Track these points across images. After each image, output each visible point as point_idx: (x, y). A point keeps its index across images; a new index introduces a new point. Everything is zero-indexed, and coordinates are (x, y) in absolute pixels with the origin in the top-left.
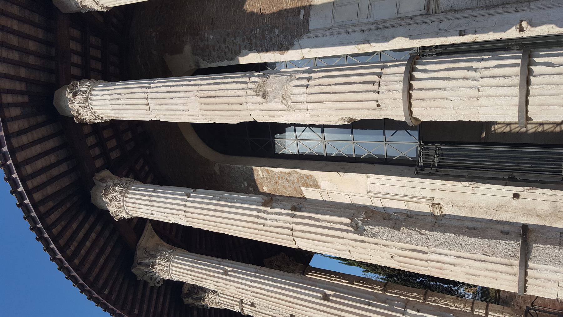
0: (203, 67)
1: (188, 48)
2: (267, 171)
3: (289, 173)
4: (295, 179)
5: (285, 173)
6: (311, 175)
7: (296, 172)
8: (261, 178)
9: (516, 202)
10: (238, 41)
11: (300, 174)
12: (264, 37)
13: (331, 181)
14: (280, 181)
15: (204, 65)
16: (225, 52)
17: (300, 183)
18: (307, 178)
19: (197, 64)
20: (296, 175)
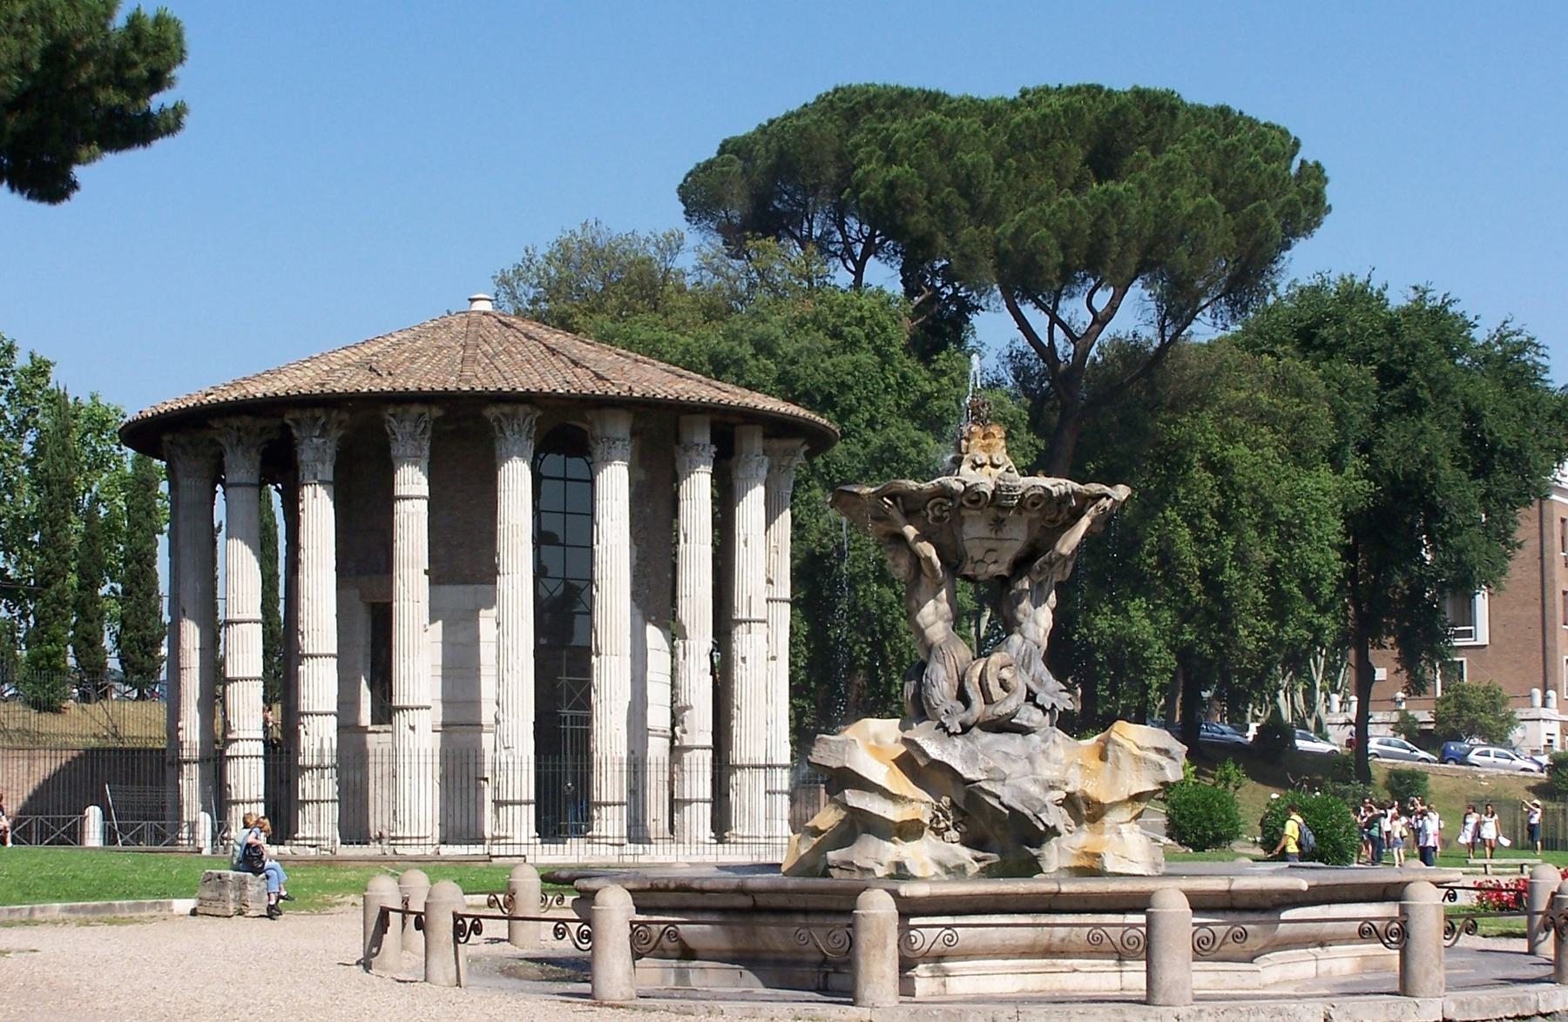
1: (642, 475)
12: (645, 576)
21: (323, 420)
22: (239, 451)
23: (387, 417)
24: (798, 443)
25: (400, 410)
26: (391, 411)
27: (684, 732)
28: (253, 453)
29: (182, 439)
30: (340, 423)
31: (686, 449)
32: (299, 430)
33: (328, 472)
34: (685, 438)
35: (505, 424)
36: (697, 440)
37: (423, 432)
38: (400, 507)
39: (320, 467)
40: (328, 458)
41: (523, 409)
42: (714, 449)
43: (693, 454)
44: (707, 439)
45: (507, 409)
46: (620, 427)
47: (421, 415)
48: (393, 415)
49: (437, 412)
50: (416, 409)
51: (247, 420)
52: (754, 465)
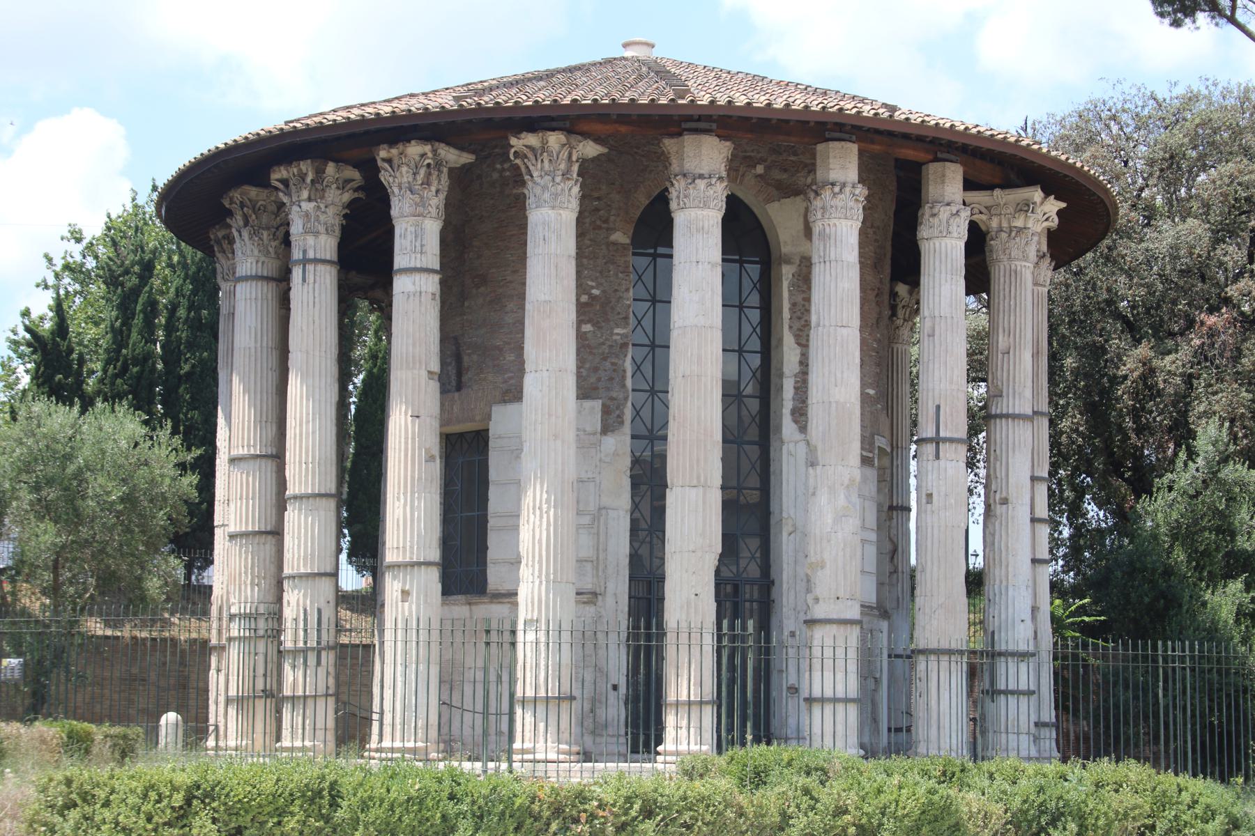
0: (784, 271)
2: (624, 346)
3: (624, 386)
4: (614, 395)
5: (624, 378)
6: (622, 423)
7: (626, 399)
8: (612, 329)
11: (624, 405)
13: (616, 454)
14: (608, 364)
16: (799, 318)
17: (609, 403)
18: (619, 416)
19: (788, 262)
20: (621, 396)
22: (245, 234)
23: (380, 163)
25: (394, 151)
26: (383, 154)
27: (817, 600)
32: (289, 195)
33: (326, 246)
36: (833, 176)
37: (427, 183)
38: (402, 285)
39: (311, 240)
40: (322, 229)
41: (555, 139)
42: (862, 191)
43: (827, 194)
44: (852, 174)
45: (532, 139)
46: (707, 156)
47: (423, 155)
48: (389, 161)
49: (453, 157)
50: (415, 149)
51: (253, 192)
52: (944, 213)
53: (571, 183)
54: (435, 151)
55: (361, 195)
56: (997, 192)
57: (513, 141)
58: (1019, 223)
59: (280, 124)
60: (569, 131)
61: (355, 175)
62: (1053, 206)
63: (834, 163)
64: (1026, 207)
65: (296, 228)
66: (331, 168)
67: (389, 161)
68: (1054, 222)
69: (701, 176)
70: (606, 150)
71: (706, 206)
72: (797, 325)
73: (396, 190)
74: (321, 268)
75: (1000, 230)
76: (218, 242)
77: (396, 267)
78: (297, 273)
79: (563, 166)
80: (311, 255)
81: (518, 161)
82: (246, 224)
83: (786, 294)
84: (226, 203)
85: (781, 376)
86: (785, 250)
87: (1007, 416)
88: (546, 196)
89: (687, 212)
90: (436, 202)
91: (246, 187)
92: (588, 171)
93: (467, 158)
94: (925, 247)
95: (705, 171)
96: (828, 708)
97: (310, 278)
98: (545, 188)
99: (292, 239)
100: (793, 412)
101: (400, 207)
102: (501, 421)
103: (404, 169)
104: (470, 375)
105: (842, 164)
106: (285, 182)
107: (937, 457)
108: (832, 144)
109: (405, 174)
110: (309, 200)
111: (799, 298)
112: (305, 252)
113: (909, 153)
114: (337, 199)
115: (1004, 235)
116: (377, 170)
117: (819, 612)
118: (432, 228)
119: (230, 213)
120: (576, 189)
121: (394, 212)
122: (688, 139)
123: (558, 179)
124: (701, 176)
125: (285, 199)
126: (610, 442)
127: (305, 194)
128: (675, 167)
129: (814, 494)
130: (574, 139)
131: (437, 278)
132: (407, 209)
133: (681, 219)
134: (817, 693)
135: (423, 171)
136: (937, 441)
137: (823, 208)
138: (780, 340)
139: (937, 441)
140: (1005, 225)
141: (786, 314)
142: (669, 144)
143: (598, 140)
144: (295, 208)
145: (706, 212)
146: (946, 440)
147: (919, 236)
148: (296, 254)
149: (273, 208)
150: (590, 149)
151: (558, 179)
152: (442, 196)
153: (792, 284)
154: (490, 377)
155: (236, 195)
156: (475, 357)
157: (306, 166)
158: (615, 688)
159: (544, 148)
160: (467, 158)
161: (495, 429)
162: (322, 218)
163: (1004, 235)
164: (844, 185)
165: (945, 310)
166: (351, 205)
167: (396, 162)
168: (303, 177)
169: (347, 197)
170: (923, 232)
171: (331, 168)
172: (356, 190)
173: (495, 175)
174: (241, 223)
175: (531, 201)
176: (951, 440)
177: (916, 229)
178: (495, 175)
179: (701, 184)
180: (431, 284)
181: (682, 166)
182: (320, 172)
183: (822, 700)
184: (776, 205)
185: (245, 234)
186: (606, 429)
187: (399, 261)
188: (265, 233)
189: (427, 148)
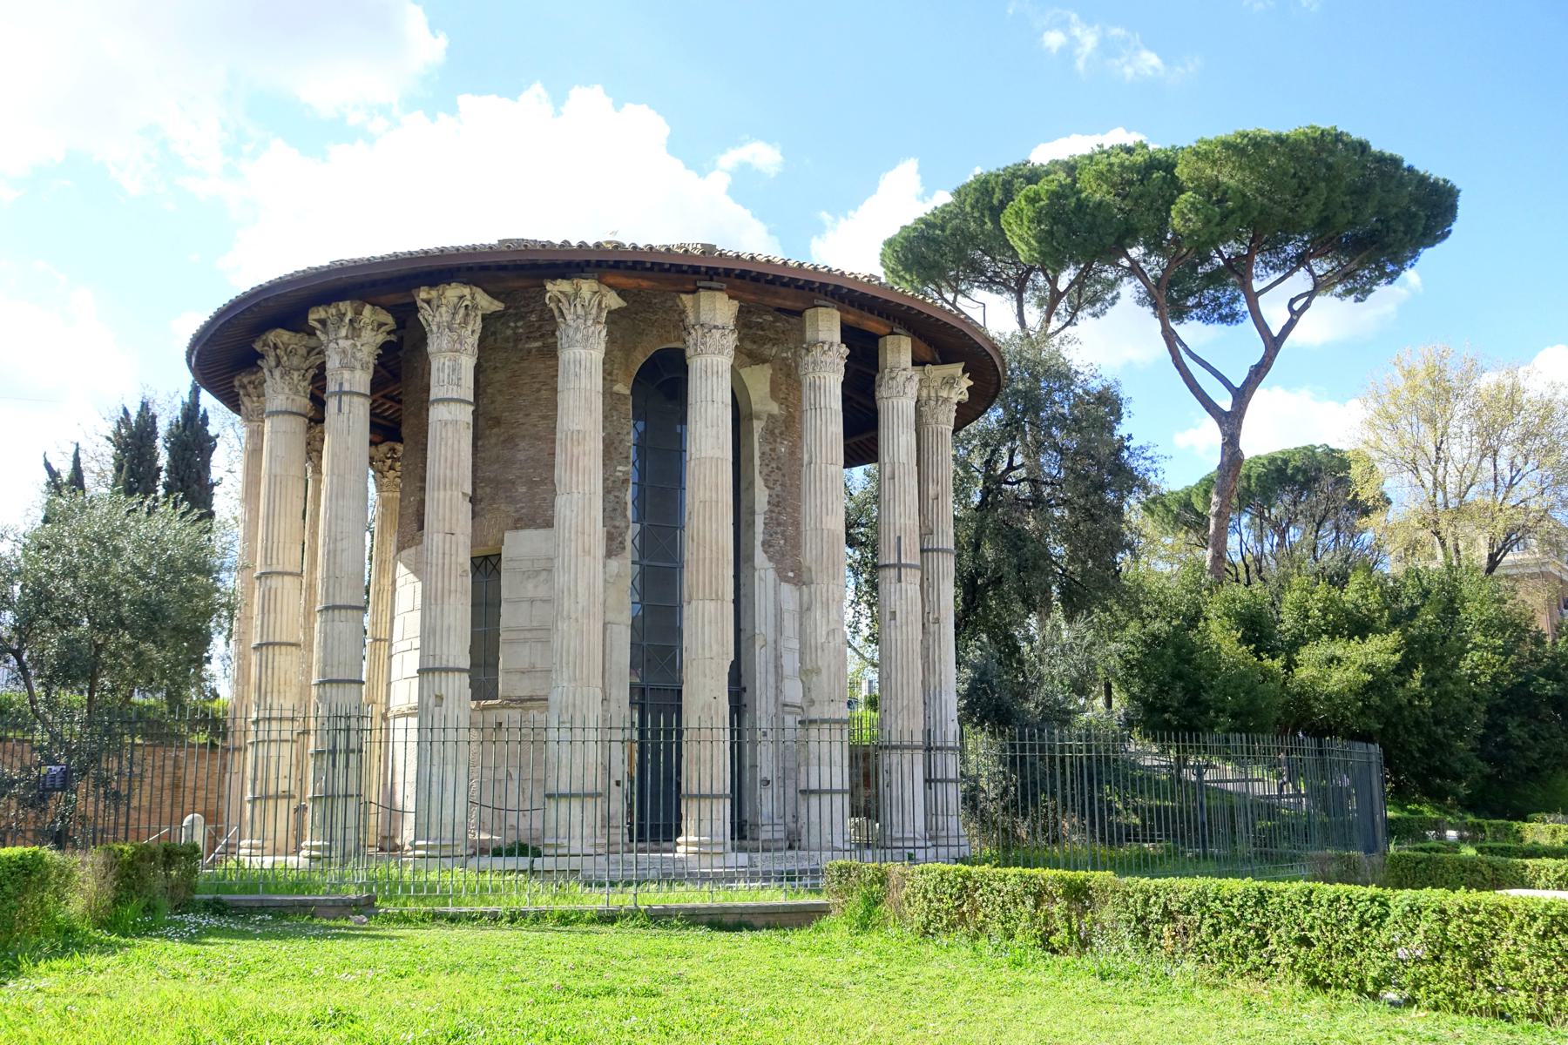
1: (774, 408)
2: (626, 481)
5: (625, 509)
9: (613, 783)
10: (778, 488)
12: (779, 524)
13: (618, 575)
15: (758, 426)
19: (758, 418)
21: (349, 316)
22: (277, 373)
23: (420, 303)
24: (957, 369)
25: (434, 293)
28: (296, 375)
29: (245, 380)
30: (381, 325)
31: (808, 350)
32: (326, 333)
33: (361, 380)
34: (809, 335)
35: (565, 306)
36: (822, 336)
38: (437, 414)
39: (347, 374)
41: (587, 287)
42: (845, 351)
43: (816, 352)
44: (837, 337)
45: (564, 286)
47: (461, 297)
48: (428, 302)
50: (453, 292)
52: (901, 379)
53: (600, 327)
54: (473, 298)
55: (393, 338)
56: (929, 367)
57: (549, 286)
58: (944, 394)
59: (326, 263)
60: (600, 281)
61: (389, 319)
62: (966, 383)
63: (823, 325)
64: (950, 382)
65: (333, 363)
66: (367, 310)
67: (428, 302)
68: (965, 397)
69: (716, 327)
70: (623, 304)
71: (721, 353)
72: (765, 471)
73: (435, 328)
74: (356, 399)
75: (929, 398)
76: (244, 387)
77: (432, 397)
78: (332, 405)
79: (594, 311)
80: (346, 387)
81: (552, 305)
82: (278, 364)
83: (756, 445)
84: (258, 346)
85: (753, 513)
86: (756, 407)
87: (938, 550)
88: (579, 336)
89: (704, 358)
90: (472, 340)
91: (279, 331)
92: (614, 318)
93: (498, 306)
94: (882, 405)
95: (719, 323)
96: (826, 798)
97: (345, 408)
98: (577, 329)
99: (328, 374)
100: (763, 543)
101: (438, 344)
102: (519, 546)
103: (443, 309)
104: (483, 505)
105: (827, 326)
106: (323, 322)
107: (900, 580)
108: (820, 310)
109: (444, 315)
110: (346, 337)
111: (767, 449)
112: (341, 385)
113: (872, 324)
114: (369, 342)
115: (932, 403)
116: (417, 310)
117: (814, 714)
118: (468, 363)
119: (262, 356)
120: (604, 333)
121: (431, 348)
122: (703, 294)
123: (590, 323)
124: (716, 327)
125: (323, 337)
126: (614, 564)
127: (343, 332)
128: (691, 319)
129: (809, 609)
130: (605, 289)
131: (471, 408)
132: (445, 345)
133: (696, 364)
134: (814, 785)
135: (462, 311)
136: (899, 566)
137: (815, 363)
138: (752, 483)
139: (899, 566)
140: (933, 394)
141: (757, 461)
142: (683, 296)
143: (621, 293)
144: (332, 345)
145: (719, 358)
146: (906, 566)
147: (878, 395)
148: (332, 386)
149: (303, 351)
150: (614, 301)
151: (590, 323)
152: (477, 336)
153: (761, 436)
154: (503, 507)
155: (272, 336)
156: (488, 490)
157: (346, 307)
158: (618, 783)
159: (576, 295)
160: (498, 306)
161: (506, 553)
162: (359, 355)
163: (932, 403)
164: (831, 344)
165: (903, 458)
166: (385, 346)
167: (435, 303)
168: (342, 316)
169: (381, 338)
170: (882, 393)
171: (367, 310)
172: (389, 333)
173: (509, 332)
174: (273, 364)
175: (563, 341)
176: (911, 566)
177: (874, 392)
178: (509, 332)
179: (717, 334)
180: (465, 414)
181: (697, 316)
182: (358, 313)
183: (819, 792)
184: (748, 370)
185: (277, 373)
186: (609, 554)
187: (435, 393)
188: (296, 375)
189: (466, 291)
